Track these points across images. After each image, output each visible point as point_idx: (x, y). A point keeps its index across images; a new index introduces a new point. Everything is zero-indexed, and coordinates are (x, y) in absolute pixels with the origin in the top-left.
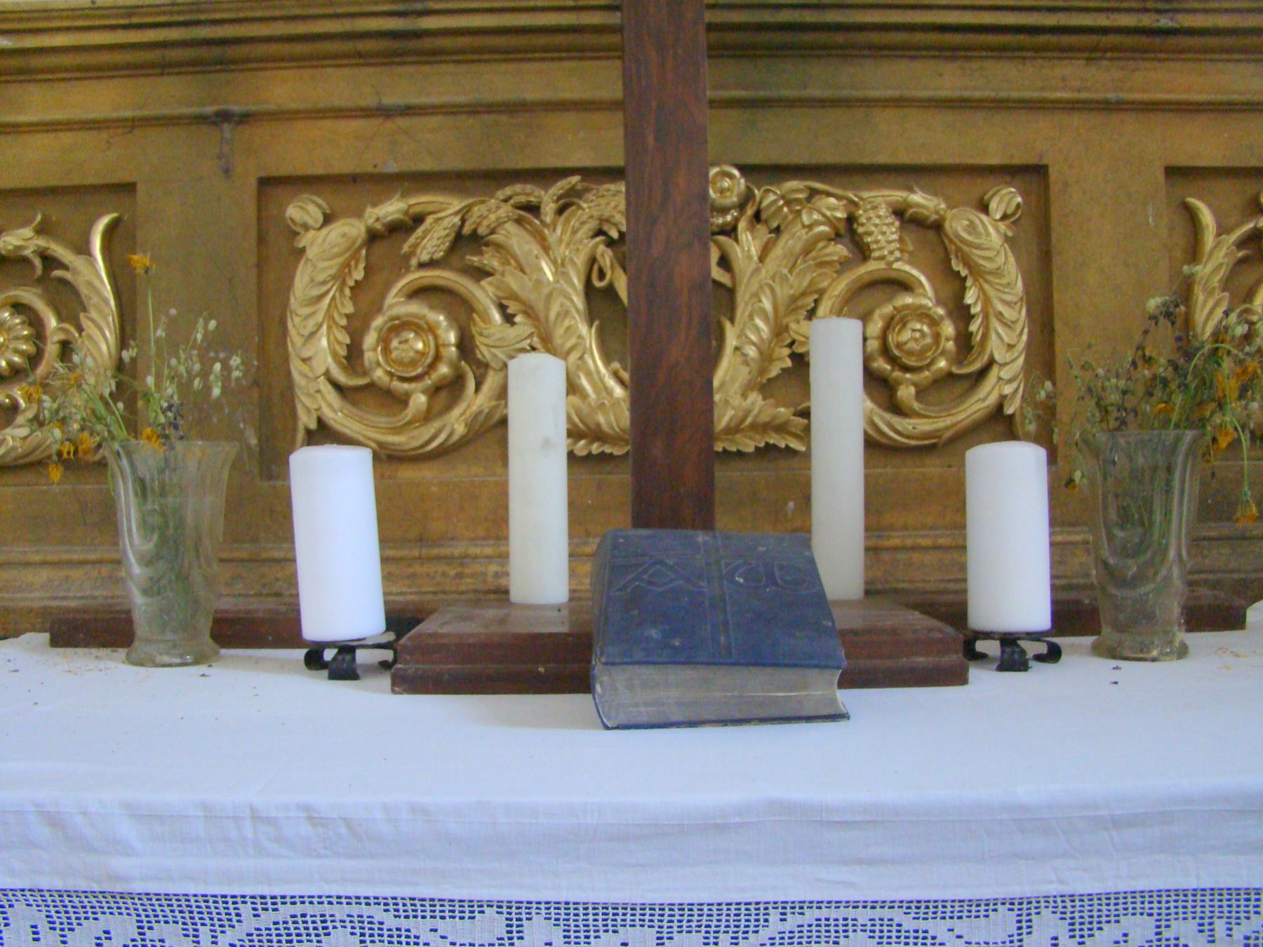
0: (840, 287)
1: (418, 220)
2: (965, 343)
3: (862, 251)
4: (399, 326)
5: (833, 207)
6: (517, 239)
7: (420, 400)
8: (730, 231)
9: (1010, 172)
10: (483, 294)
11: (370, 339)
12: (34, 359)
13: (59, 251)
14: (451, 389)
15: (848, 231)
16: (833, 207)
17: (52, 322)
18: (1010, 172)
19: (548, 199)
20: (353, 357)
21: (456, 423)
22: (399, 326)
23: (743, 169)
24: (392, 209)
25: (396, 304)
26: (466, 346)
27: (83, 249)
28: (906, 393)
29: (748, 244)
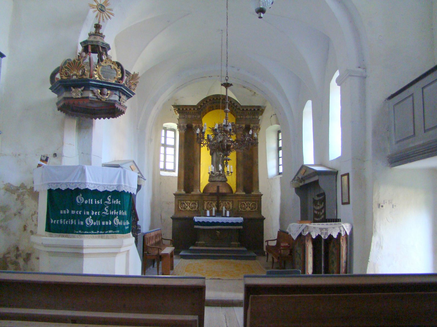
0: (225, 205)
1: (209, 202)
2: (230, 207)
3: (226, 204)
4: (209, 206)
5: (225, 202)
6: (213, 203)
7: (209, 209)
8: (221, 203)
9: (231, 201)
10: (212, 205)
11: (207, 206)
12: (194, 207)
13: (195, 202)
14: (210, 209)
15: (225, 203)
16: (225, 202)
17: (195, 205)
18: (231, 201)
19: (214, 202)
20: (207, 207)
21: (211, 209)
22: (209, 206)
23: (222, 201)
24: (208, 202)
25: (208, 205)
26: (211, 207)
27: (196, 202)
28: (227, 209)
29: (221, 203)
